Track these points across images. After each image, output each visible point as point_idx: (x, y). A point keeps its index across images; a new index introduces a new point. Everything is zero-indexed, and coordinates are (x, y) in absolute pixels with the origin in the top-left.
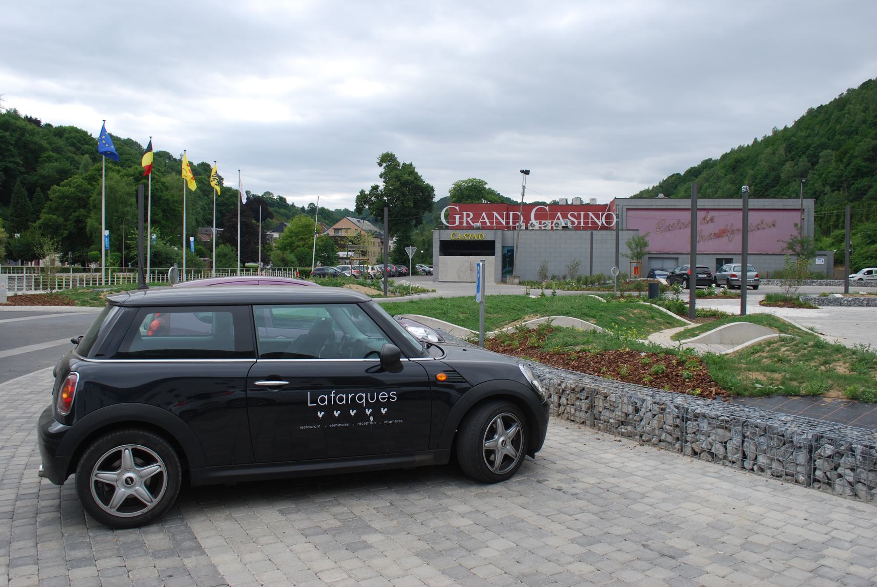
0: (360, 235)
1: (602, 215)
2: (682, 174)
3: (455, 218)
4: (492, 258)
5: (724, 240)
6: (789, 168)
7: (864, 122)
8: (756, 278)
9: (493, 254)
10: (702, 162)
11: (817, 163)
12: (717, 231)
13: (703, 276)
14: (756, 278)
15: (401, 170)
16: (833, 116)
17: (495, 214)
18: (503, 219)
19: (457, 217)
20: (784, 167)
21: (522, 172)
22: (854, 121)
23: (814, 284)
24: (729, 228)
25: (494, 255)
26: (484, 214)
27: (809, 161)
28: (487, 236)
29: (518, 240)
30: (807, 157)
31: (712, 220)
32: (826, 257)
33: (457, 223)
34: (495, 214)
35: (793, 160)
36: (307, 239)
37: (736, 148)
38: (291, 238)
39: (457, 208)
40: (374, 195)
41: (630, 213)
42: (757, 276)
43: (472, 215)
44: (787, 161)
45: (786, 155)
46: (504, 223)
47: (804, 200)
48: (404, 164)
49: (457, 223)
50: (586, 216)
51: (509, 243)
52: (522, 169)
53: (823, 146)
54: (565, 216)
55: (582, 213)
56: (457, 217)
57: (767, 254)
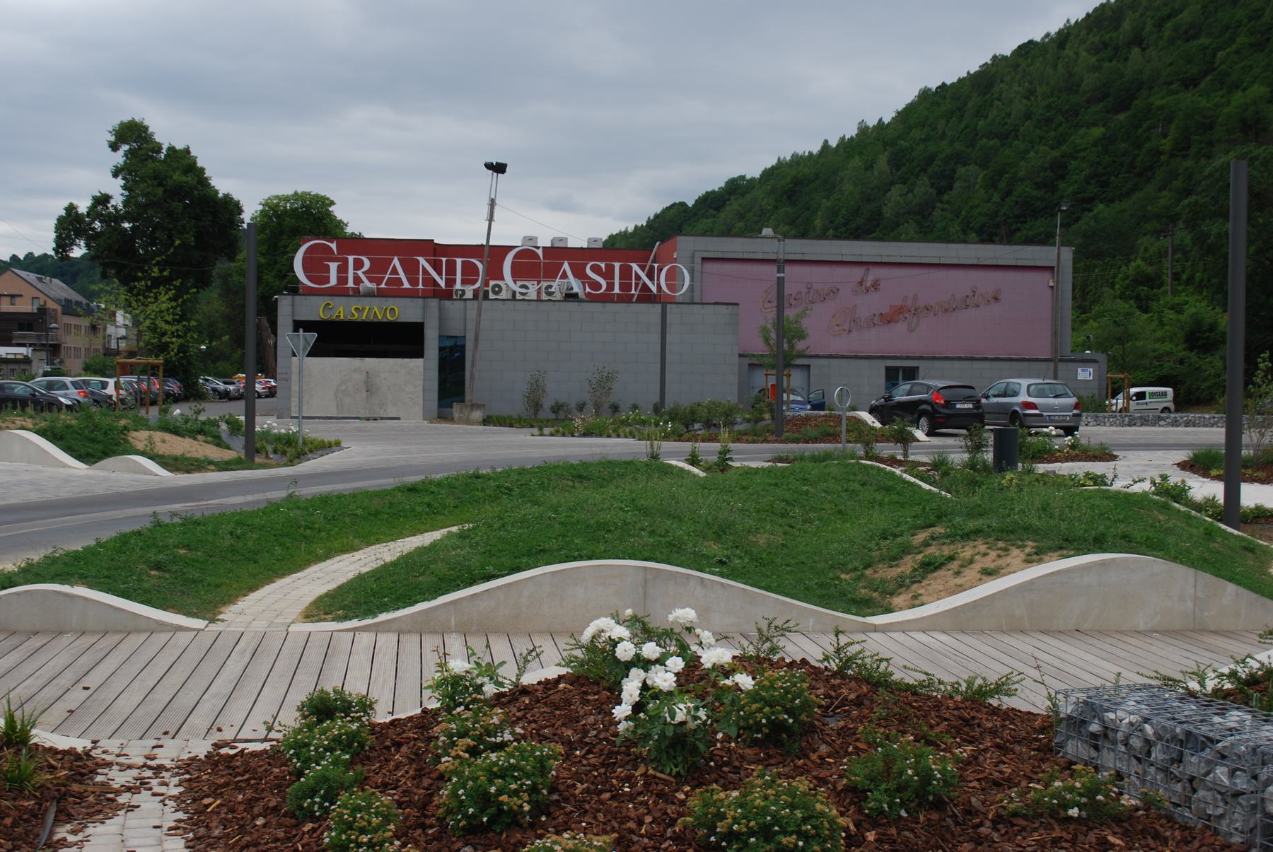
0: (43, 311)
1: (660, 270)
2: (690, 203)
3: (328, 269)
4: (420, 361)
5: (900, 328)
6: (898, 198)
7: (1028, 116)
8: (1075, 411)
9: (419, 354)
10: (727, 183)
11: (950, 187)
12: (885, 310)
13: (966, 406)
14: (1075, 411)
15: (164, 161)
16: (970, 105)
17: (422, 261)
18: (440, 274)
19: (333, 267)
20: (889, 194)
21: (489, 166)
22: (1009, 114)
23: (1162, 423)
24: (909, 303)
25: (422, 357)
26: (396, 261)
27: (932, 185)
28: (406, 311)
29: (478, 323)
30: (930, 178)
31: (875, 286)
32: (1096, 365)
33: (333, 281)
34: (422, 261)
35: (904, 183)
37: (788, 158)
39: (333, 246)
40: (99, 216)
41: (709, 267)
42: (1077, 406)
43: (367, 264)
44: (892, 183)
45: (891, 173)
46: (442, 283)
47: (1063, 249)
48: (172, 150)
49: (333, 281)
50: (626, 273)
51: (455, 329)
52: (489, 160)
53: (959, 159)
54: (579, 273)
55: (617, 265)
56: (333, 267)
57: (985, 359)
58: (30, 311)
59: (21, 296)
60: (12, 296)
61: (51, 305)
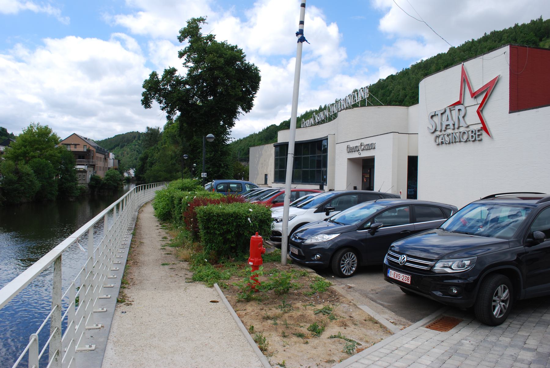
0: (89, 151)
16: (380, 93)
22: (399, 95)
36: (43, 149)
37: (309, 111)
38: (25, 147)
58: (83, 151)
59: (79, 145)
60: (76, 145)
61: (91, 148)
